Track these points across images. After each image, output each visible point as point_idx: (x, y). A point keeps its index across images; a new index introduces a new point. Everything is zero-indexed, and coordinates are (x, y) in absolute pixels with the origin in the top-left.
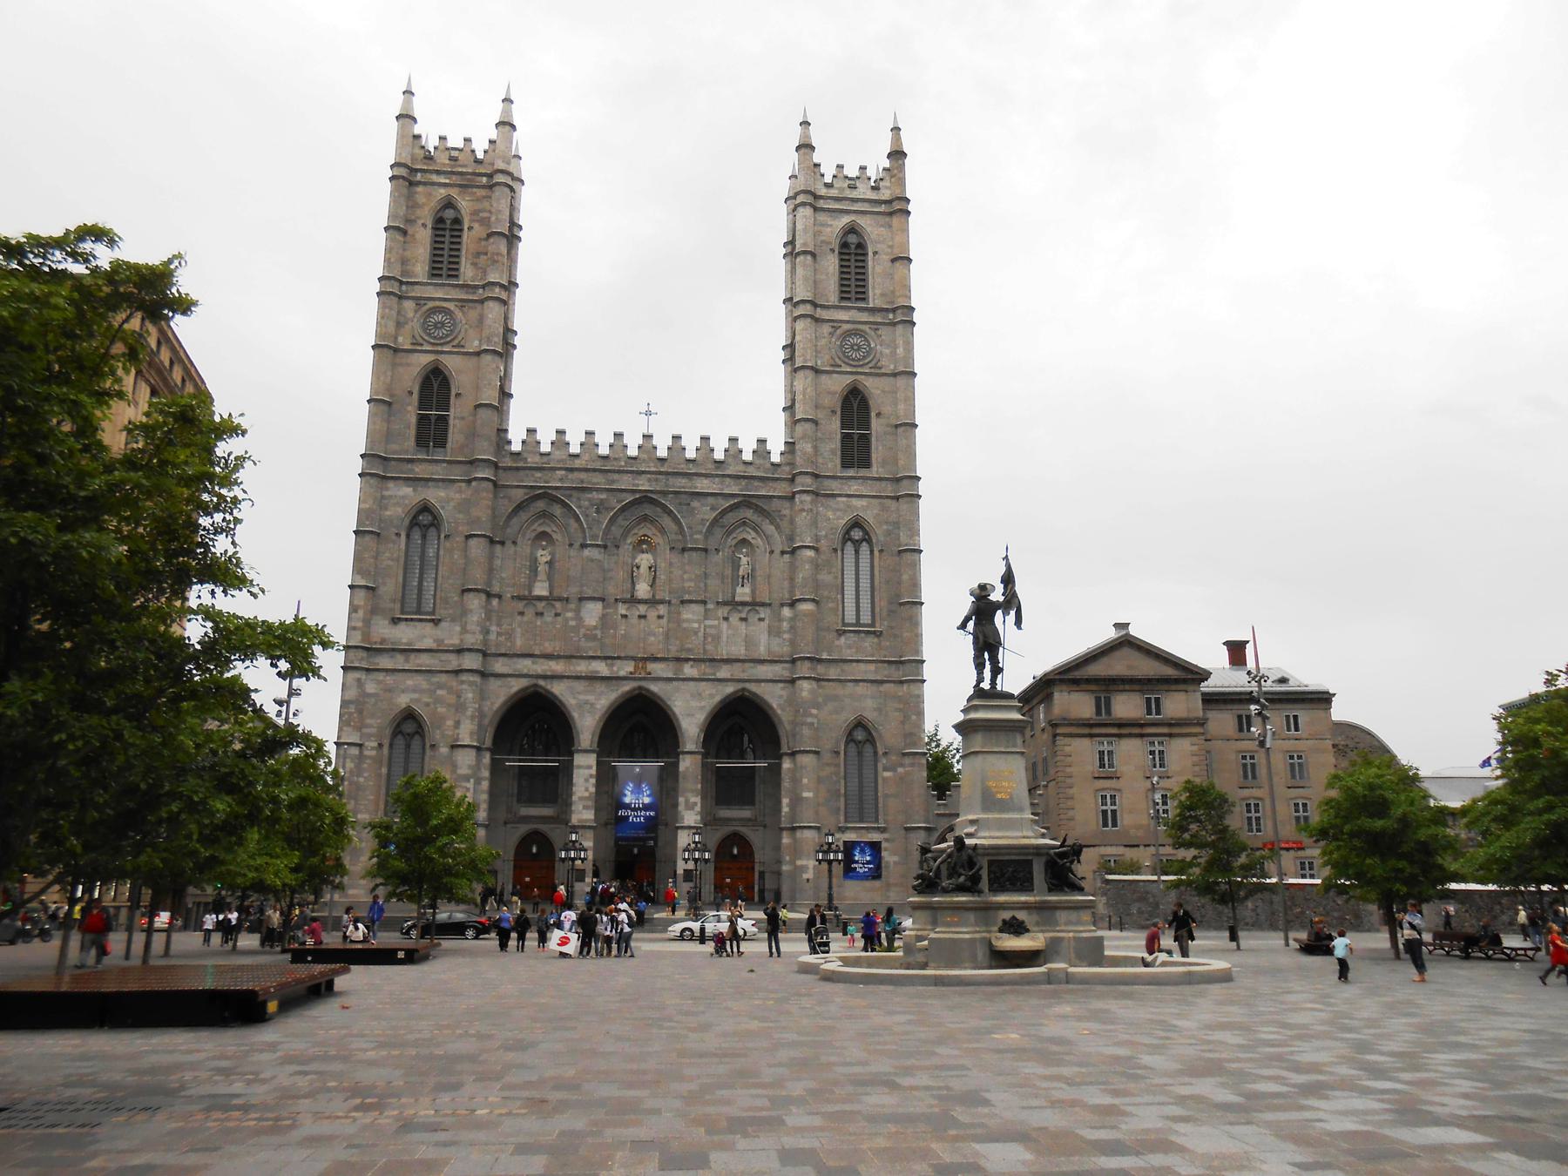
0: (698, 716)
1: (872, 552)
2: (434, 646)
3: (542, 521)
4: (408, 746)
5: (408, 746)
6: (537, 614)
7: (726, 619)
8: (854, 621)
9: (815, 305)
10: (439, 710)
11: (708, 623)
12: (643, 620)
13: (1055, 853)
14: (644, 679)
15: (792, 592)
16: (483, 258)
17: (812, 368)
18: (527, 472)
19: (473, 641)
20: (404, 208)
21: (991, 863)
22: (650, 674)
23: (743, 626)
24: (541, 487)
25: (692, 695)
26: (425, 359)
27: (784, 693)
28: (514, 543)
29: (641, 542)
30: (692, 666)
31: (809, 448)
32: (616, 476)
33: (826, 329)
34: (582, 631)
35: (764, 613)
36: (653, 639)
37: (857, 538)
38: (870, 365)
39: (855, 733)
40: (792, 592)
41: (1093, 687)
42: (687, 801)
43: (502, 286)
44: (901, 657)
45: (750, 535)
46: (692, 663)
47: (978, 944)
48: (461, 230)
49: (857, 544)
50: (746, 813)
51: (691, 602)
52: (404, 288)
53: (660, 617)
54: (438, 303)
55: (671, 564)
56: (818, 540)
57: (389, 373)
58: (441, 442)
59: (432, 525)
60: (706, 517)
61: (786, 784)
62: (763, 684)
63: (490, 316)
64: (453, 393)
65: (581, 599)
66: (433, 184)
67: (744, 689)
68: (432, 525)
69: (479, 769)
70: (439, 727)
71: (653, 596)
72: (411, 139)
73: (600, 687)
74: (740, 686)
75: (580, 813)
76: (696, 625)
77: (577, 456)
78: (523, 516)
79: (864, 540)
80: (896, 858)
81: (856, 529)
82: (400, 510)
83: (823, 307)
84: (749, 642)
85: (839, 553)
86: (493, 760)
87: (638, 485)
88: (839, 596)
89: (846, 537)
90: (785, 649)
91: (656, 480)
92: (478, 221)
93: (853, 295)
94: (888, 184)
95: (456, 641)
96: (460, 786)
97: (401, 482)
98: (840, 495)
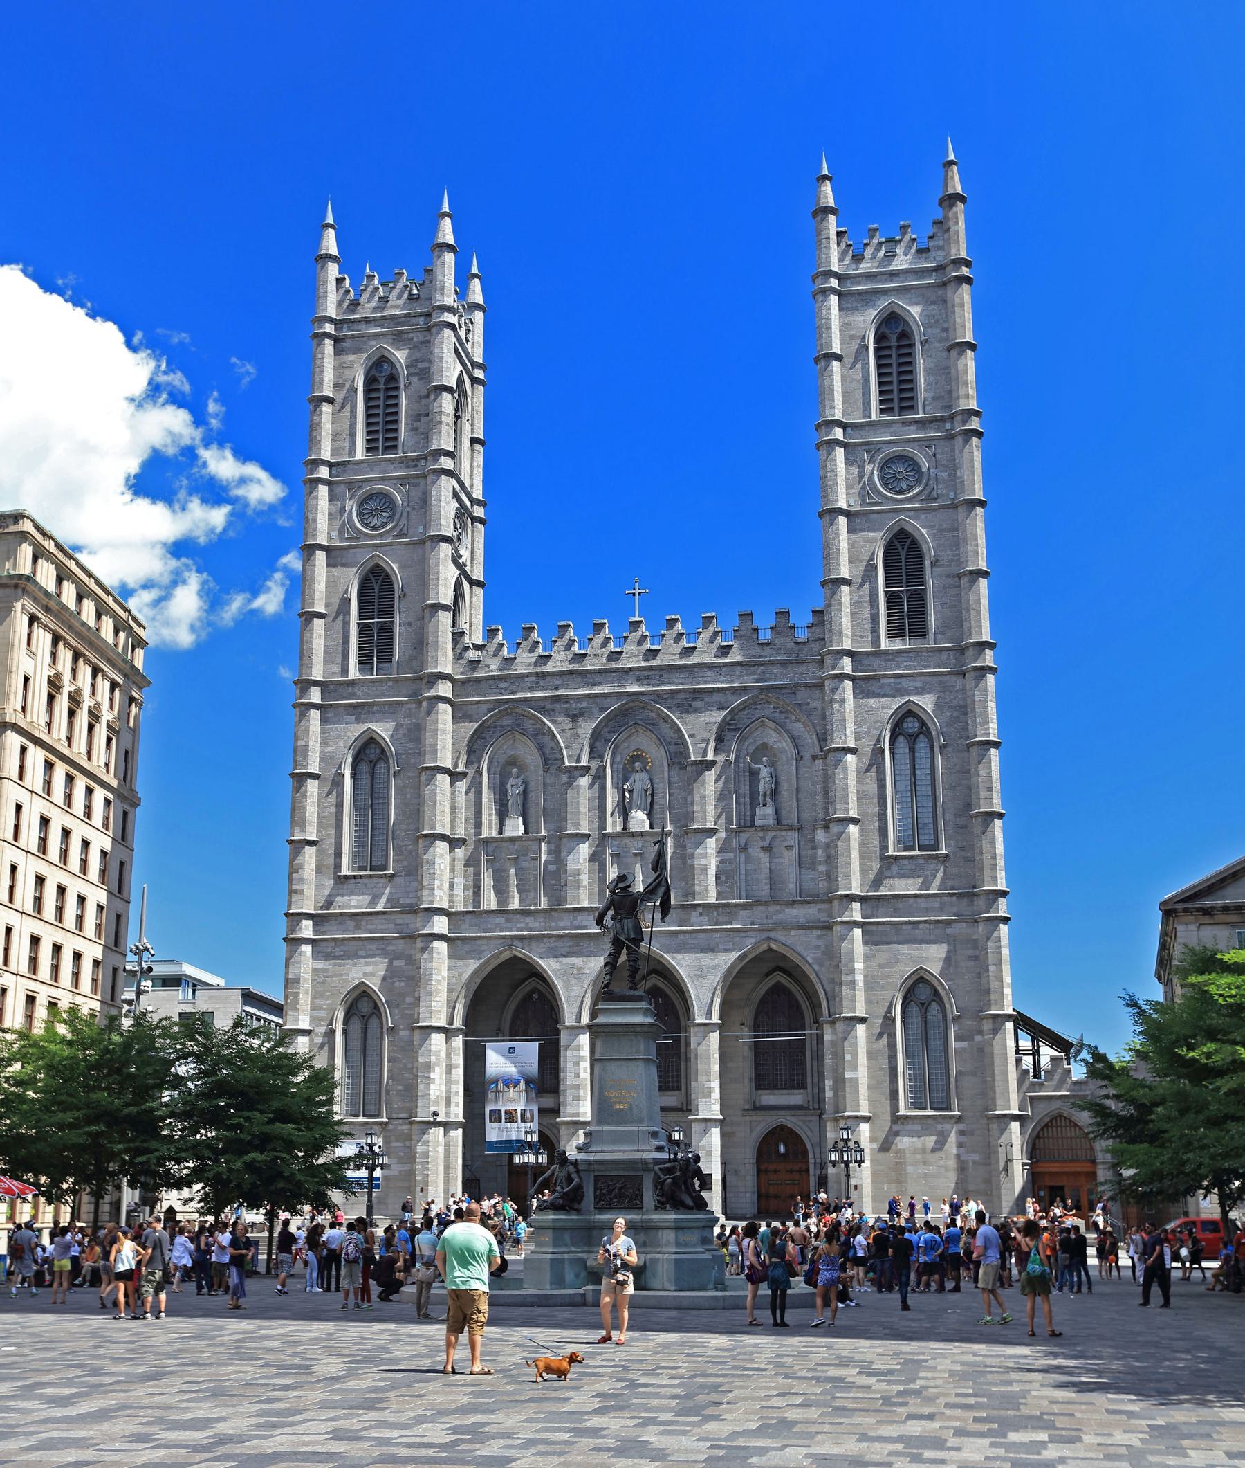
1: (932, 748)
10: (397, 984)
13: (661, 1169)
15: (826, 810)
16: (423, 419)
18: (491, 682)
21: (597, 1179)
23: (764, 858)
27: (821, 943)
29: (635, 758)
30: (701, 914)
35: (791, 838)
39: (917, 991)
40: (826, 810)
41: (1234, 918)
43: (449, 454)
44: (975, 887)
45: (773, 737)
46: (700, 910)
47: (567, 1266)
48: (397, 388)
49: (912, 739)
50: (796, 1098)
55: (670, 783)
56: (857, 739)
60: (713, 720)
61: (828, 1061)
62: (793, 933)
63: (434, 493)
64: (396, 595)
66: (362, 336)
67: (769, 938)
74: (765, 935)
76: (703, 861)
80: (976, 1157)
81: (911, 719)
82: (341, 744)
84: (775, 880)
86: (466, 1043)
90: (821, 885)
91: (648, 677)
92: (417, 374)
93: (896, 405)
94: (941, 243)
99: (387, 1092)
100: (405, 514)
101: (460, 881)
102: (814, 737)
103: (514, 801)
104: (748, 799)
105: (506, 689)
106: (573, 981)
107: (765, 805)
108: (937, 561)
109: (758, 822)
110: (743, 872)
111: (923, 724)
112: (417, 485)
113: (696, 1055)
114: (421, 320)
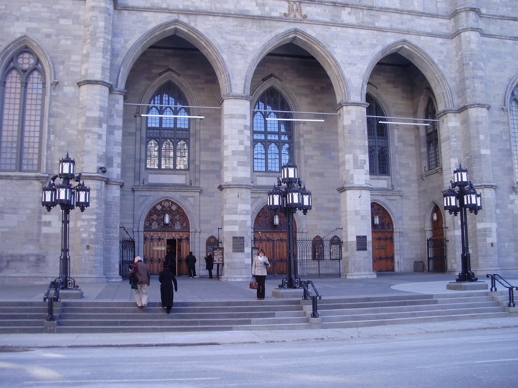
0: (360, 66)
4: (25, 85)
5: (25, 85)
10: (63, 42)
14: (300, 21)
22: (306, 16)
25: (352, 43)
27: (443, 48)
30: (349, 14)
42: (355, 159)
46: (348, 10)
62: (422, 38)
67: (405, 41)
69: (111, 116)
70: (63, 63)
73: (250, 27)
74: (401, 37)
75: (234, 169)
96: (90, 132)
99: (49, 148)
106: (238, 57)
113: (350, 132)
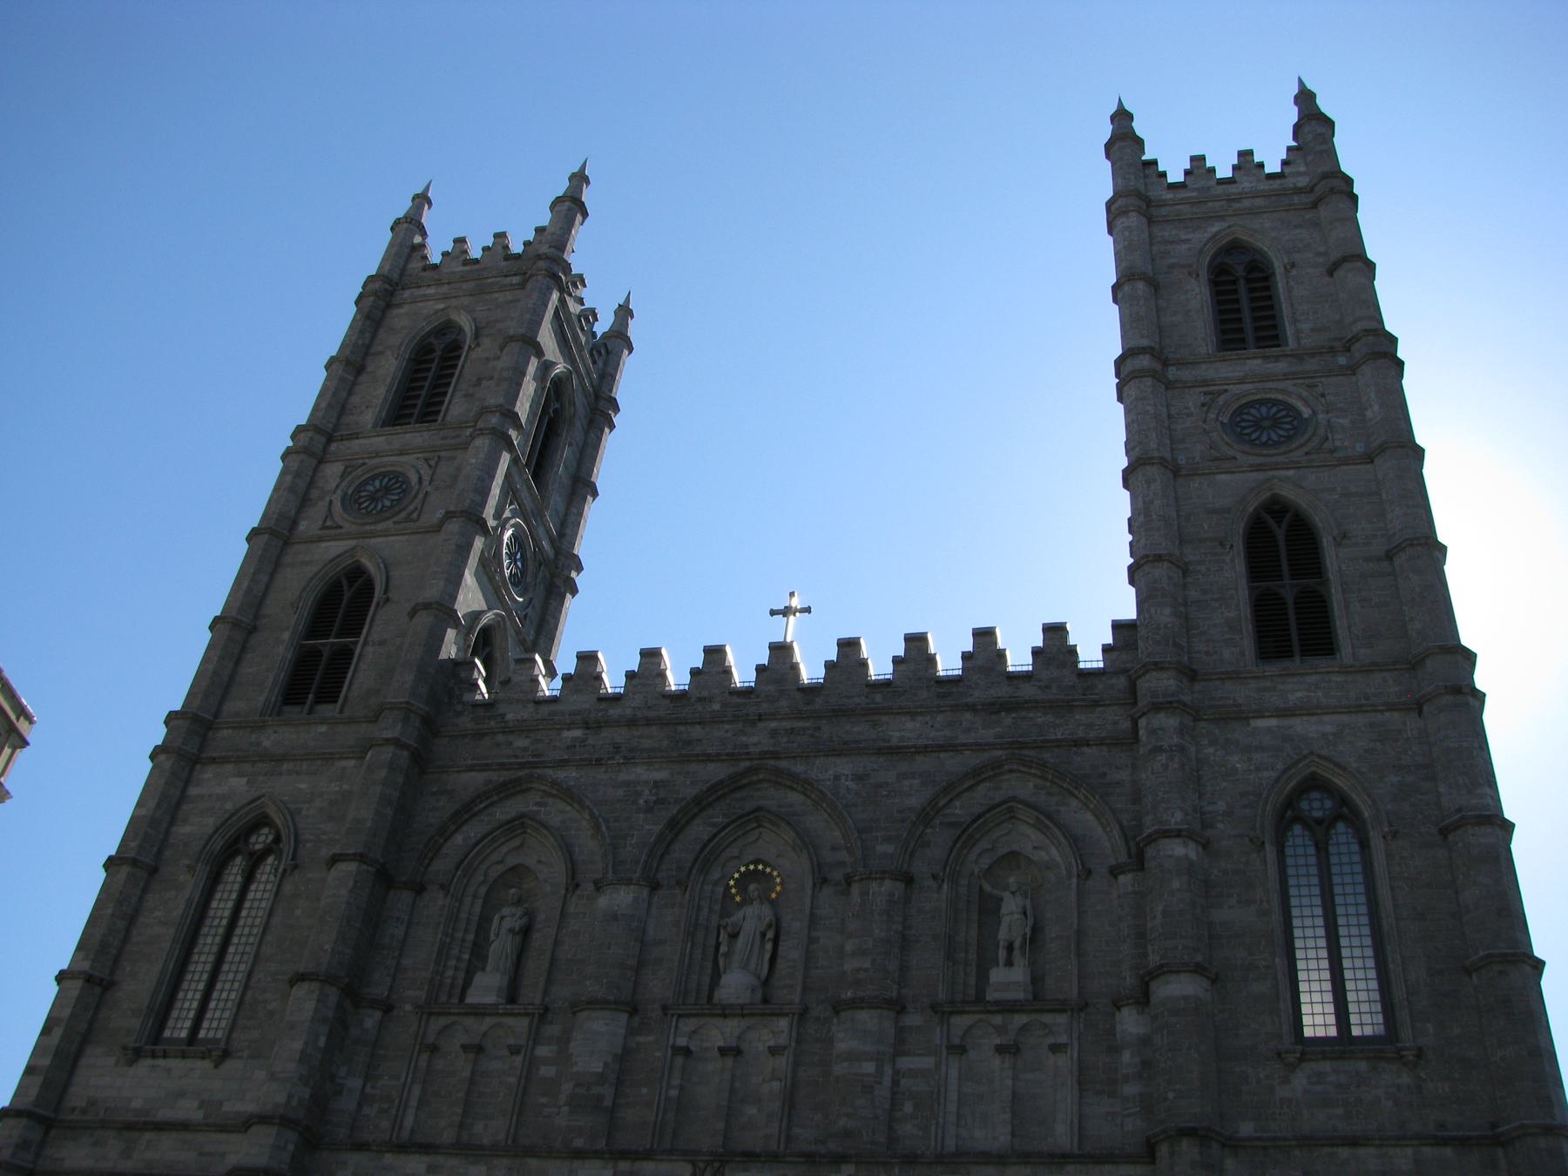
1: (1364, 845)
2: (198, 1116)
3: (516, 842)
6: (465, 1048)
7: (960, 1050)
8: (1333, 1032)
9: (1165, 363)
11: (905, 1063)
12: (729, 1062)
17: (1163, 462)
18: (500, 738)
19: (281, 1098)
20: (367, 335)
24: (522, 766)
26: (334, 548)
28: (442, 887)
31: (1165, 615)
32: (697, 731)
33: (1193, 400)
34: (567, 1087)
36: (754, 1111)
37: (1318, 814)
38: (1306, 449)
45: (1027, 837)
49: (1320, 832)
51: (856, 1004)
52: (333, 447)
53: (774, 1051)
54: (386, 459)
55: (813, 920)
57: (264, 578)
58: (330, 693)
59: (267, 851)
65: (576, 1007)
68: (267, 851)
71: (765, 1000)
72: (407, 251)
76: (869, 1068)
77: (616, 698)
78: (473, 831)
79: (1339, 817)
81: (1315, 795)
83: (1181, 364)
85: (1270, 852)
87: (747, 746)
88: (1280, 962)
89: (1288, 815)
94: (1302, 169)
95: (249, 1107)
97: (229, 768)
98: (1260, 715)
100: (421, 496)
101: (355, 1083)
102: (1116, 833)
103: (501, 946)
104: (973, 956)
105: (525, 749)
107: (1009, 963)
108: (1345, 536)
109: (991, 995)
110: (953, 1096)
111: (1344, 800)
112: (454, 458)
114: (516, 280)
